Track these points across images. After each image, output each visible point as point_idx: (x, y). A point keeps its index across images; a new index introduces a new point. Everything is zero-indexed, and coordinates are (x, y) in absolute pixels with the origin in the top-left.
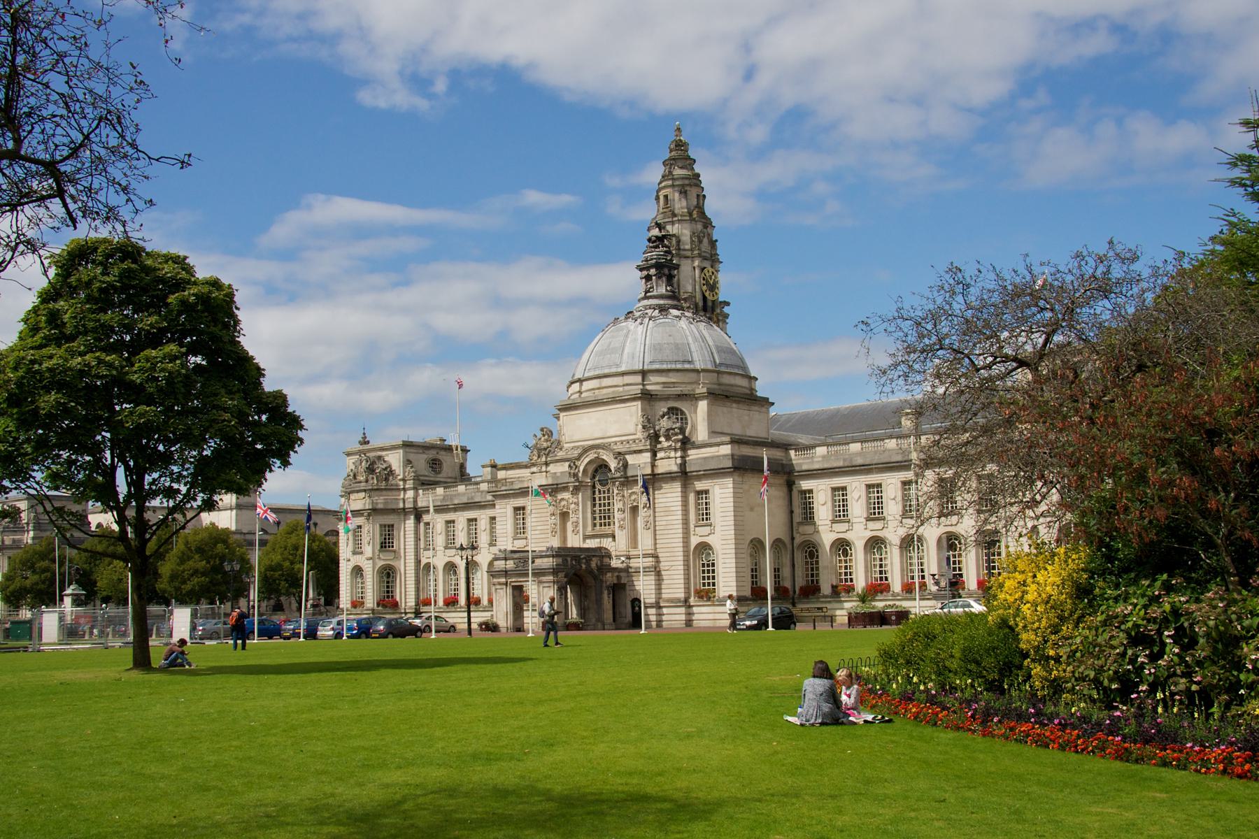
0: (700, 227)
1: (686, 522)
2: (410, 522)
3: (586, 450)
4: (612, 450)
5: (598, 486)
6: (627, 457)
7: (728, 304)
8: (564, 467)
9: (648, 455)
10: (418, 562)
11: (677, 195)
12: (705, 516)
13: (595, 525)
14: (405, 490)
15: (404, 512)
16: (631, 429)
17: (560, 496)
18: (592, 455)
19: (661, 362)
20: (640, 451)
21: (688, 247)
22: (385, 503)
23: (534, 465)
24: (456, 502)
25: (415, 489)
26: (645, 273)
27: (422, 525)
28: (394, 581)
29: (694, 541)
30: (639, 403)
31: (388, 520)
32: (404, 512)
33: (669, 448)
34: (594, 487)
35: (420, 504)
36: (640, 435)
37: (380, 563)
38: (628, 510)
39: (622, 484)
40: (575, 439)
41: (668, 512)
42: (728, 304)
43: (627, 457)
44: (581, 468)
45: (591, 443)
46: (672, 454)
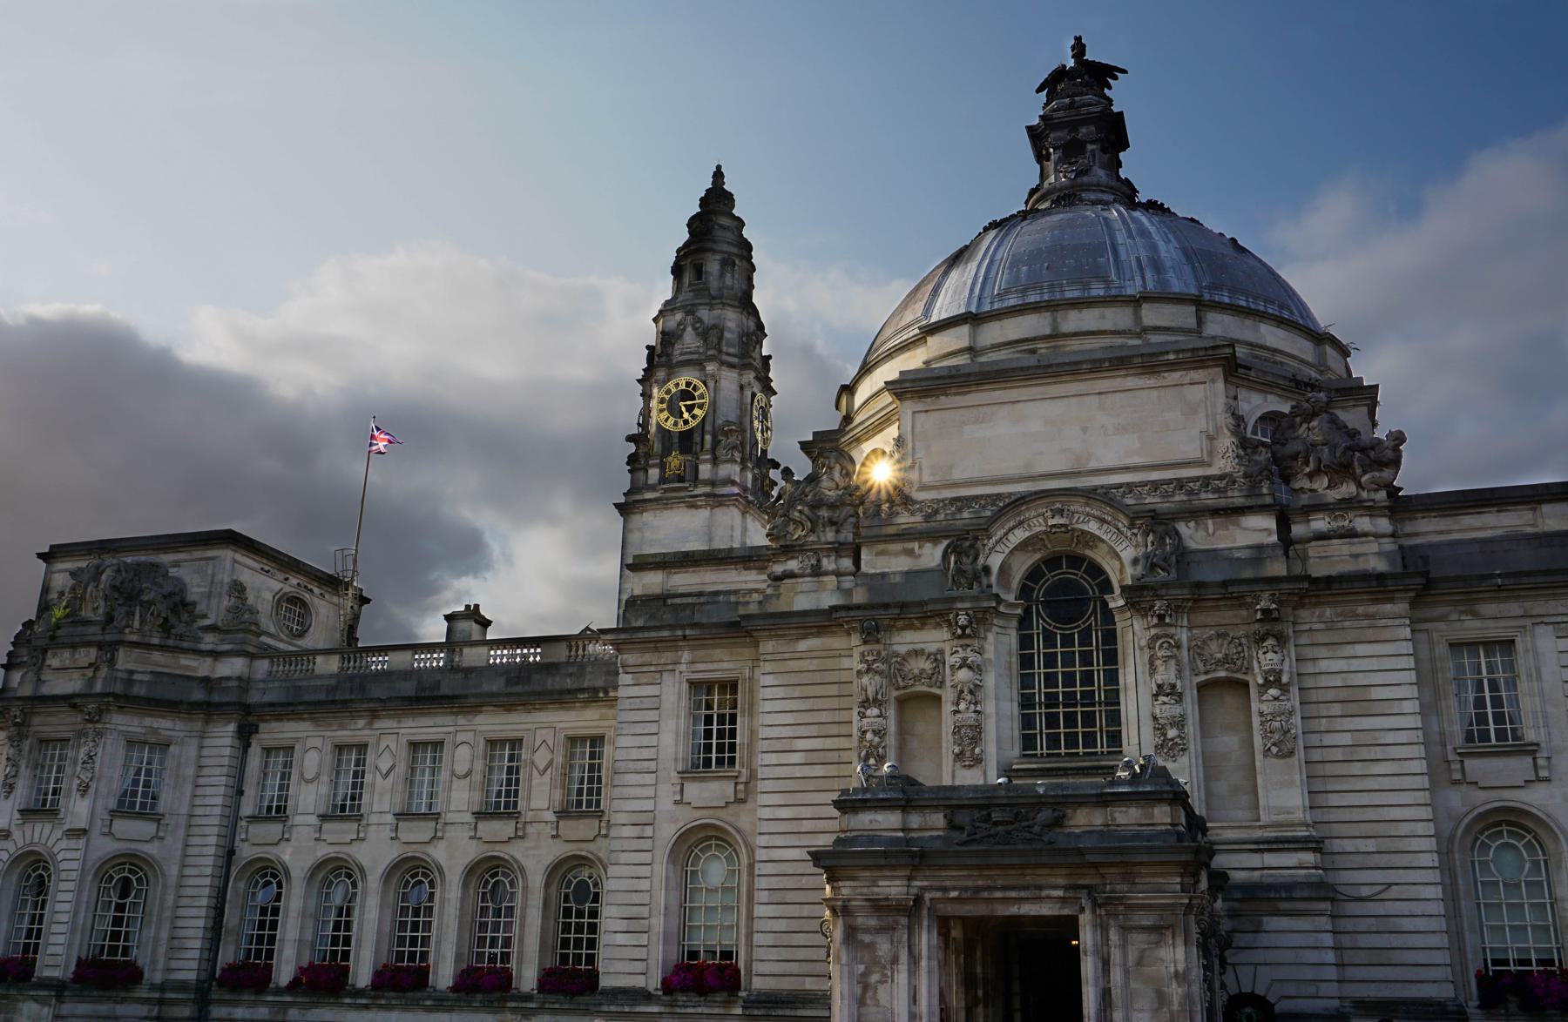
0: (752, 325)
1: (1433, 743)
6: (1182, 528)
8: (931, 555)
9: (1269, 522)
13: (1028, 742)
16: (1186, 444)
17: (904, 641)
18: (1038, 522)
21: (732, 350)
23: (788, 550)
33: (1347, 504)
36: (1224, 463)
38: (1191, 696)
39: (1177, 609)
40: (957, 475)
41: (1357, 701)
43: (1182, 528)
44: (995, 561)
45: (1021, 488)
46: (1363, 524)
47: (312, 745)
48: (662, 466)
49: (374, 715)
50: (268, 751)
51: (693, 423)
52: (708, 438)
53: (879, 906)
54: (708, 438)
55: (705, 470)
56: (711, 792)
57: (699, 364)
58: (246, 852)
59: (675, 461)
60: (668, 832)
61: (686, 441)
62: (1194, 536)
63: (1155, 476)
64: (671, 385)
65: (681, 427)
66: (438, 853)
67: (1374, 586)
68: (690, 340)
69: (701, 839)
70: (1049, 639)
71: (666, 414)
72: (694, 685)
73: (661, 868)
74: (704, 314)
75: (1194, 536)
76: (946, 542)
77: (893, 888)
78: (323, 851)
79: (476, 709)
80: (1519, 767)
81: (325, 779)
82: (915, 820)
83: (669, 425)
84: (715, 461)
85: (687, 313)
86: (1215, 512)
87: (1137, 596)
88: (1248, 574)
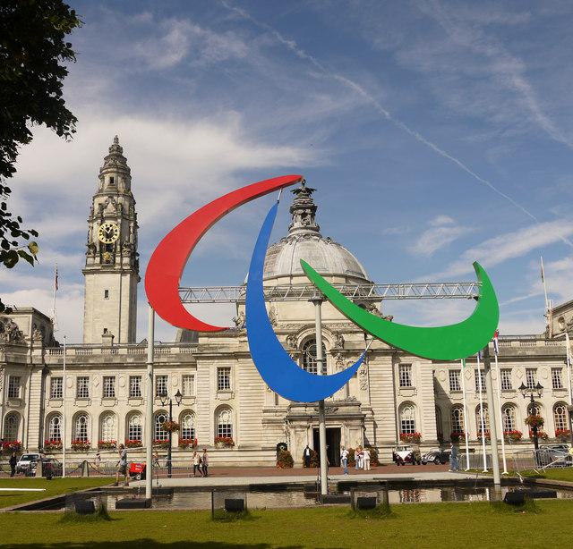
2: (37, 376)
3: (306, 327)
4: (330, 330)
5: (309, 356)
7: (138, 255)
10: (42, 410)
11: (119, 178)
12: (405, 382)
14: (32, 349)
15: (34, 367)
19: (353, 272)
20: (356, 332)
22: (16, 358)
24: (91, 362)
25: (43, 348)
26: (301, 211)
27: (48, 378)
28: (17, 427)
29: (400, 400)
30: (31, 315)
31: (18, 372)
32: (34, 367)
34: (305, 356)
35: (47, 362)
37: (9, 410)
40: (290, 318)
41: (380, 377)
42: (138, 255)
47: (69, 378)
48: (101, 258)
49: (91, 368)
50: (52, 379)
51: (113, 241)
52: (118, 247)
53: (301, 427)
54: (118, 247)
55: (118, 260)
56: (224, 397)
57: (115, 218)
58: (48, 410)
59: (106, 255)
60: (214, 407)
61: (109, 248)
62: (346, 337)
63: (337, 322)
64: (104, 225)
65: (108, 242)
66: (115, 409)
67: (384, 353)
68: (111, 208)
69: (222, 409)
70: (311, 360)
71: (102, 236)
72: (219, 369)
73: (212, 415)
74: (115, 198)
75: (346, 337)
76: (286, 336)
77: (305, 423)
78: (77, 409)
79: (126, 367)
80: (411, 392)
81: (75, 387)
82: (308, 409)
83: (104, 241)
84: (122, 257)
85: (112, 198)
86: (351, 332)
87: (334, 353)
88: (357, 348)
